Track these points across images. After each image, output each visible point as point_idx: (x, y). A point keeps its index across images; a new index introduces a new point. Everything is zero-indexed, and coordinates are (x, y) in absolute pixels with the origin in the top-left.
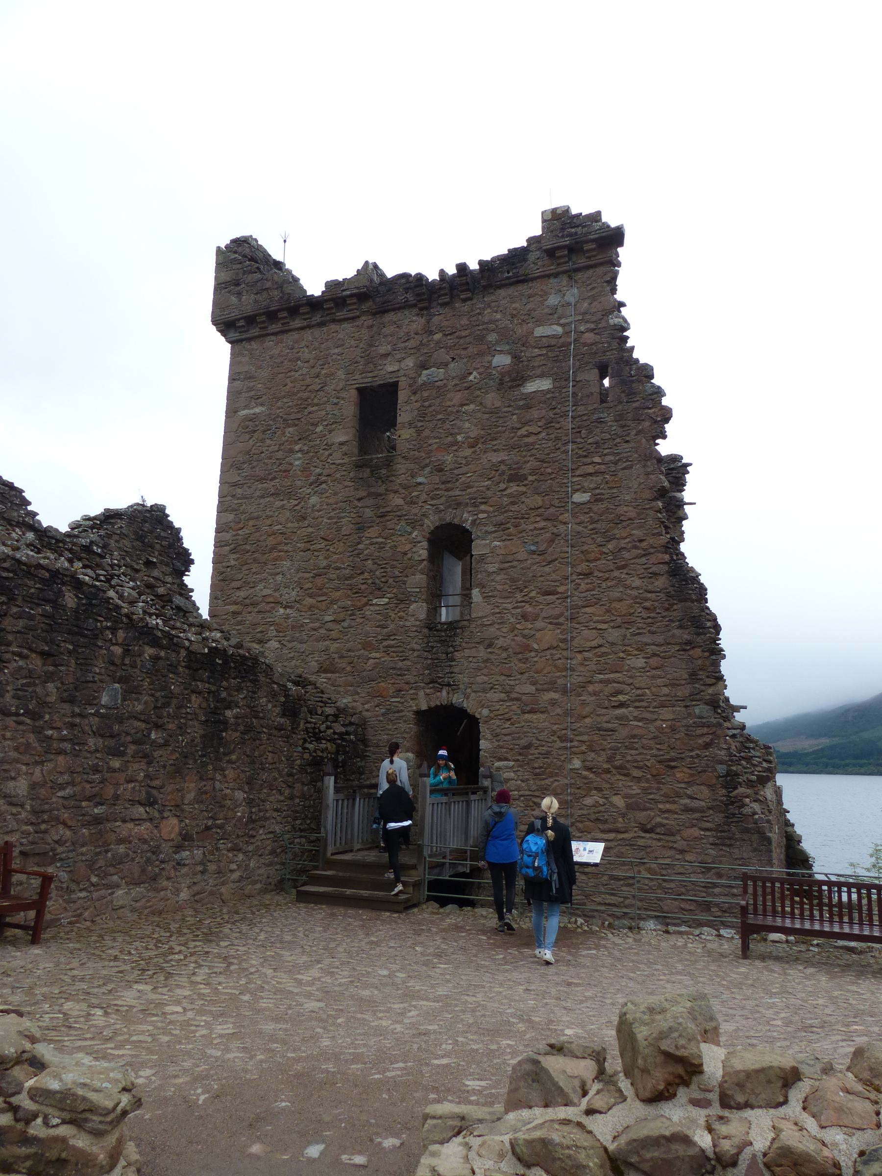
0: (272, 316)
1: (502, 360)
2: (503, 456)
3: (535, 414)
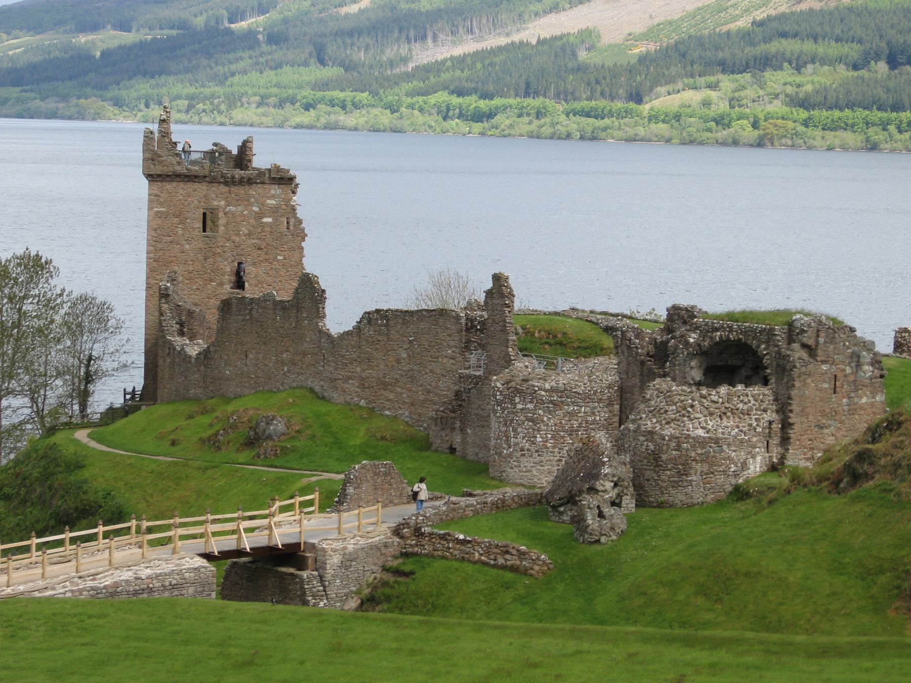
0: (168, 176)
1: (256, 209)
2: (256, 241)
3: (267, 229)
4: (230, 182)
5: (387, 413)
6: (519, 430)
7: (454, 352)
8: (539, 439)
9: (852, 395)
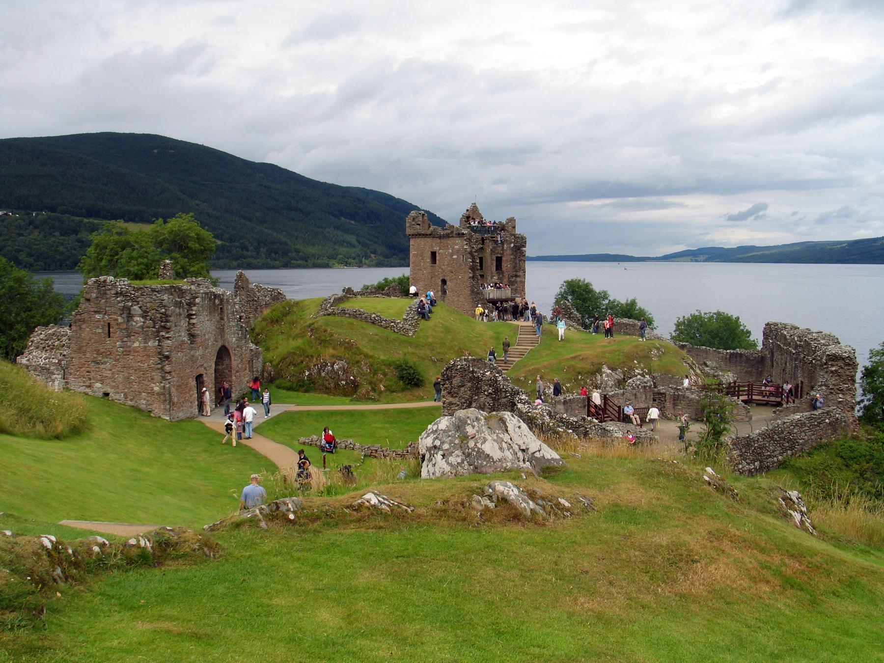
4: (440, 237)
9: (125, 339)
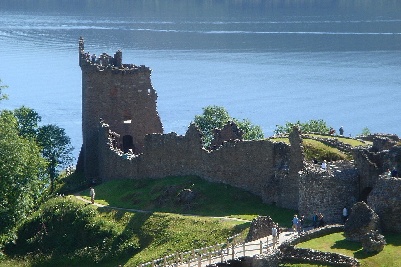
1: (134, 86)
5: (236, 186)
6: (315, 197)
7: (269, 159)
8: (325, 201)
